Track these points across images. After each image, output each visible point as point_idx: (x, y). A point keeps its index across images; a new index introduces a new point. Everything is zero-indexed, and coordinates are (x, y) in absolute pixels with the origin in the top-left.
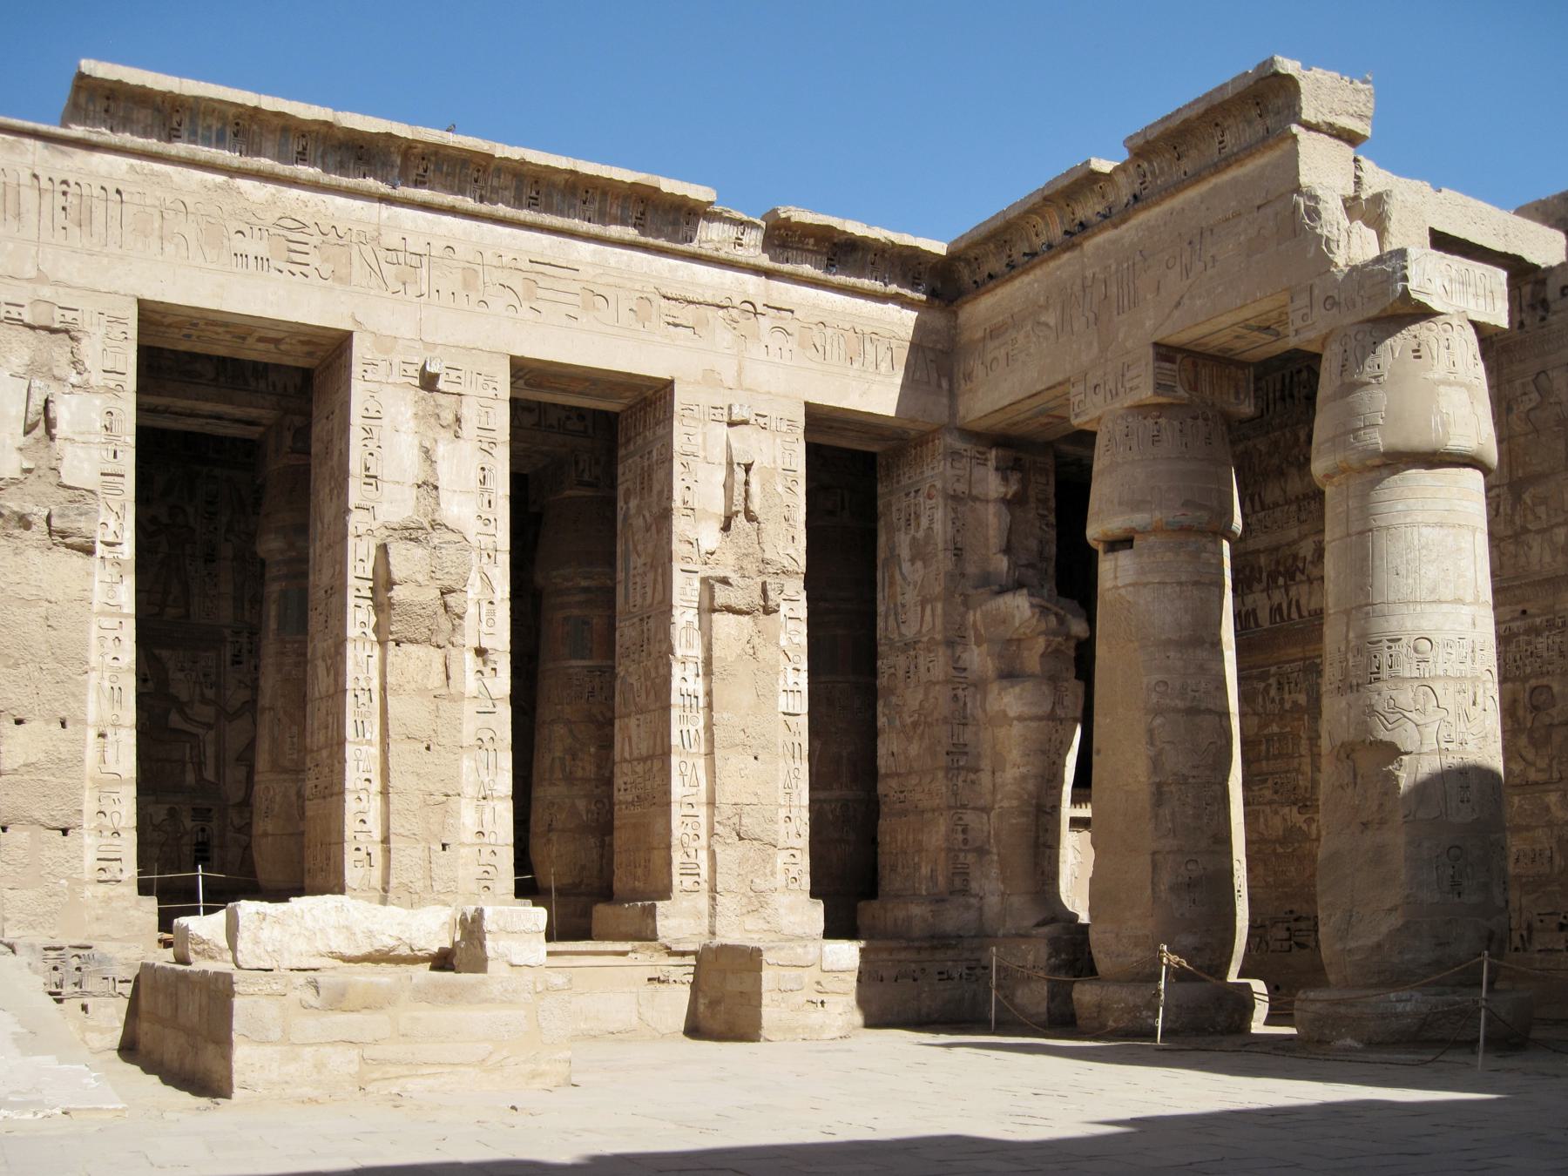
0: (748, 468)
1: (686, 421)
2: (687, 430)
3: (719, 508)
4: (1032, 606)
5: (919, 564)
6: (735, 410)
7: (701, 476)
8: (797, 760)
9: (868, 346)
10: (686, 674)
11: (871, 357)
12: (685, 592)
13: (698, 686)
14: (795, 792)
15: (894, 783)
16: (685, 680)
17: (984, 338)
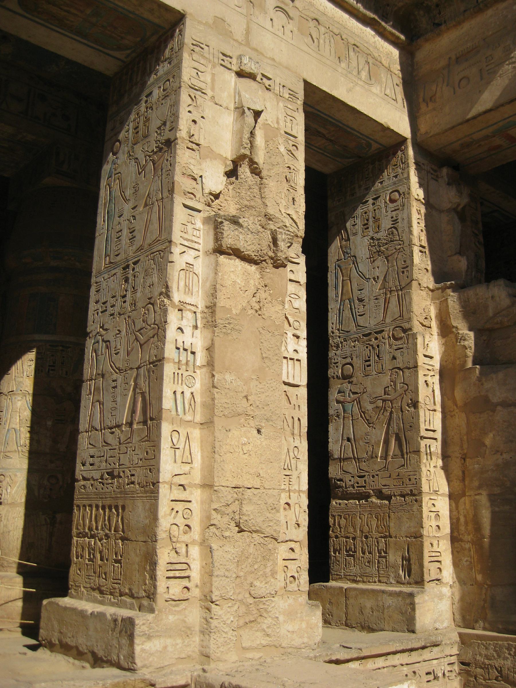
0: (257, 114)
1: (195, 56)
2: (196, 65)
3: (227, 150)
4: (510, 295)
5: (380, 261)
6: (245, 60)
7: (207, 113)
8: (297, 437)
9: (352, 53)
10: (184, 324)
11: (354, 64)
12: (189, 235)
13: (197, 340)
14: (295, 474)
15: (352, 467)
16: (183, 333)
17: (449, 65)
